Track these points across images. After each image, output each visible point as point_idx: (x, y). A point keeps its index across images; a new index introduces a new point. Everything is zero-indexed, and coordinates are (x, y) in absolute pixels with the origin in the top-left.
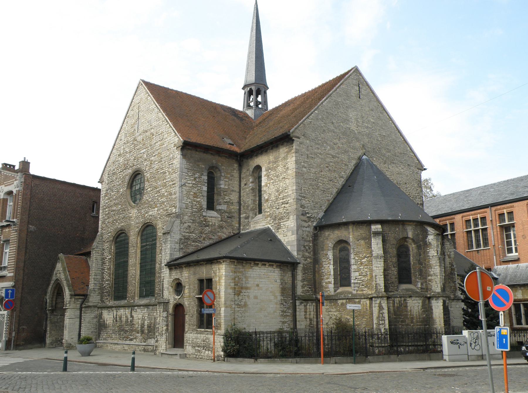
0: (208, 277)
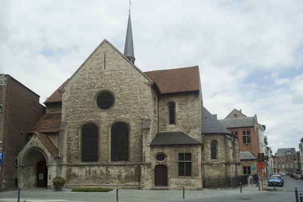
0: (188, 152)
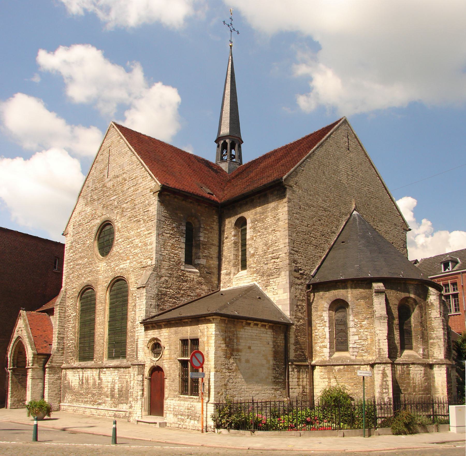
0: (194, 336)
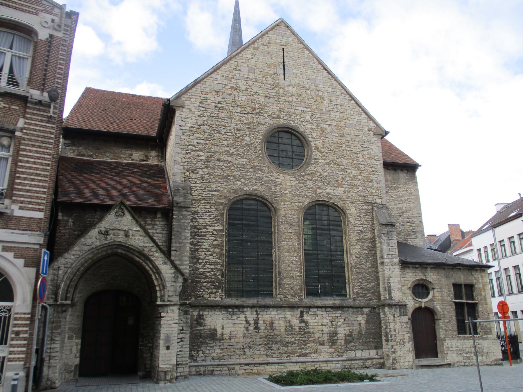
0: (468, 282)
